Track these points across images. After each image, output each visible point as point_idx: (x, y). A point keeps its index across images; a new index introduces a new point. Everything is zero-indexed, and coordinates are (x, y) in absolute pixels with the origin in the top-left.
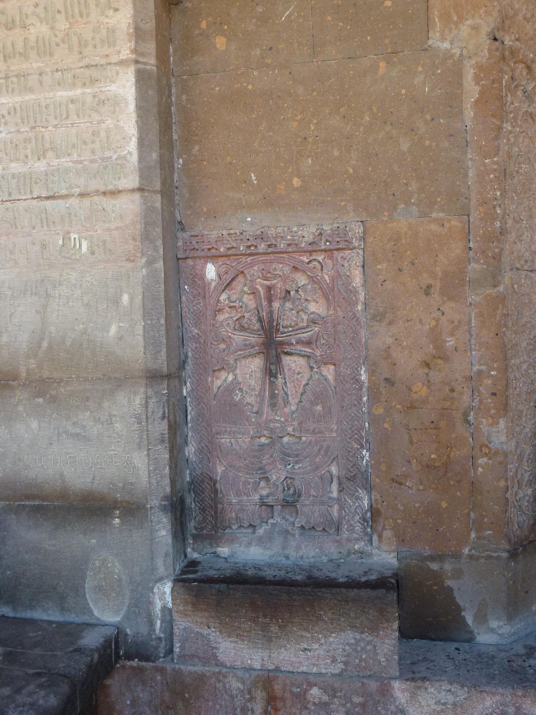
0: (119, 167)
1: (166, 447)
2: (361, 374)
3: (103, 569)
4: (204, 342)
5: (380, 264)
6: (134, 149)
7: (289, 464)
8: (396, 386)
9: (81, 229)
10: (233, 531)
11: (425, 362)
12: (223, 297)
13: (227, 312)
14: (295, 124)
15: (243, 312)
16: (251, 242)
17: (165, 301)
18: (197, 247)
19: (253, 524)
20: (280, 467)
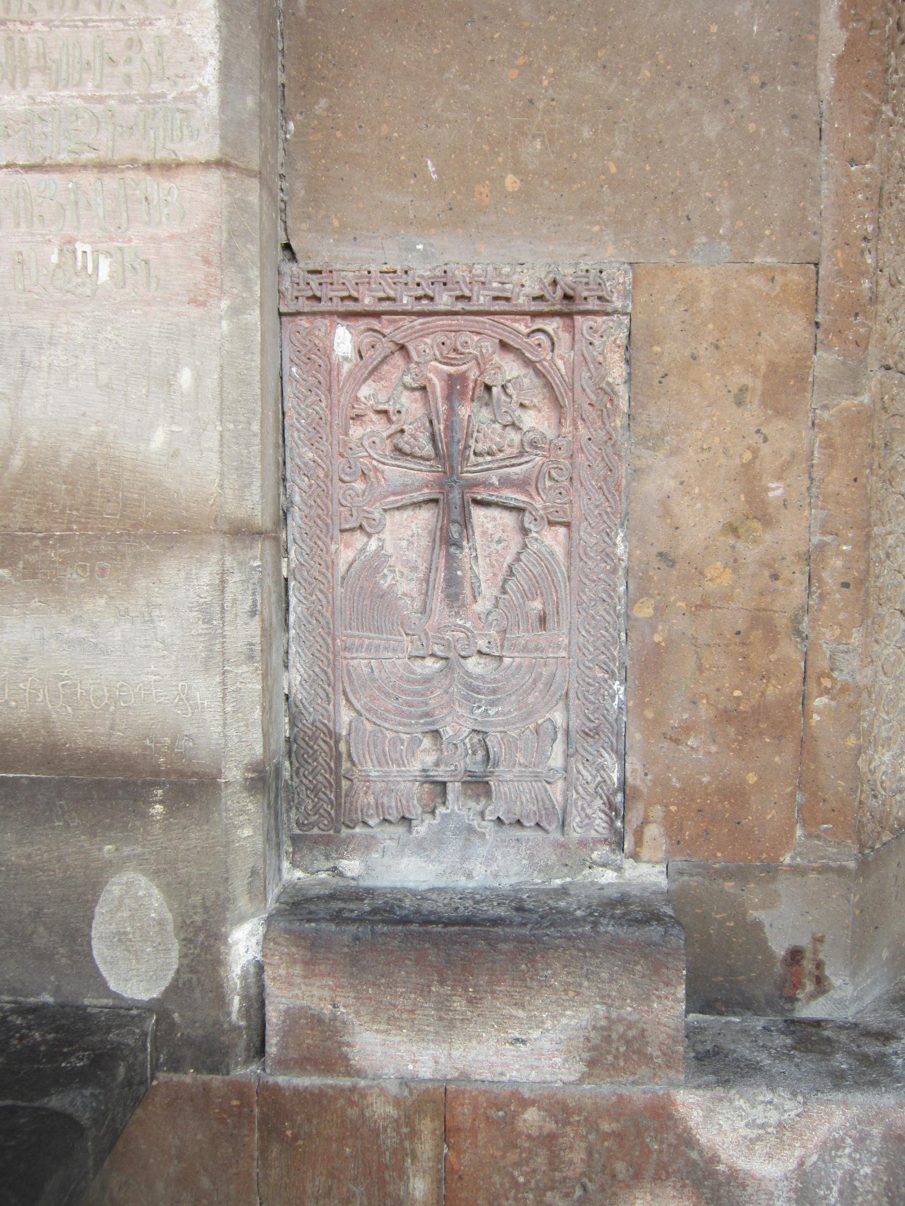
0: (178, 116)
1: (257, 669)
2: (615, 544)
3: (127, 901)
4: (326, 476)
6: (213, 81)
7: (479, 707)
8: (677, 566)
9: (98, 235)
10: (370, 830)
11: (730, 524)
12: (364, 392)
14: (514, 73)
15: (402, 423)
16: (423, 289)
17: (261, 389)
18: (318, 294)
19: (407, 815)
20: (460, 711)
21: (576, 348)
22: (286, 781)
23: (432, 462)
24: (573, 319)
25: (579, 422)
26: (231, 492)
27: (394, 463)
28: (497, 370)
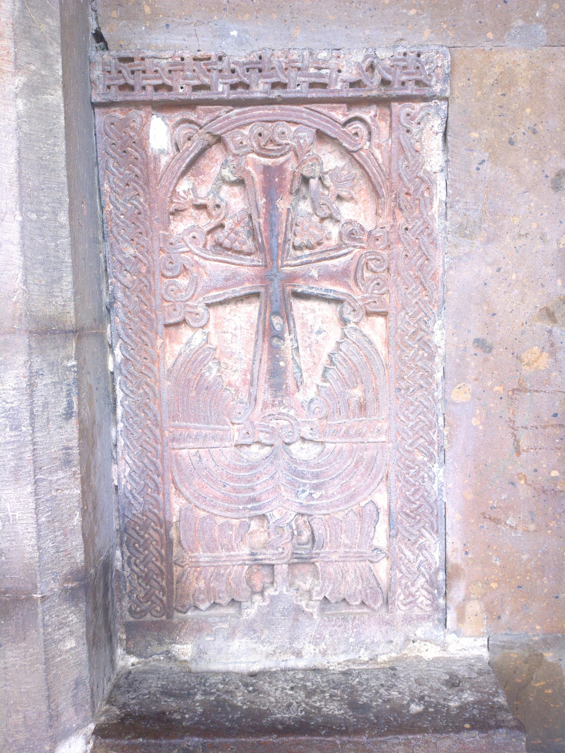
4: (148, 271)
5: (476, 129)
7: (304, 491)
8: (494, 352)
10: (202, 613)
11: (547, 309)
12: (185, 185)
13: (191, 216)
15: (222, 216)
17: (68, 177)
18: (131, 82)
19: (237, 599)
20: (286, 495)
21: (393, 137)
22: (117, 571)
23: (252, 257)
24: (389, 107)
25: (397, 211)
26: (37, 287)
27: (215, 258)
28: (315, 161)
